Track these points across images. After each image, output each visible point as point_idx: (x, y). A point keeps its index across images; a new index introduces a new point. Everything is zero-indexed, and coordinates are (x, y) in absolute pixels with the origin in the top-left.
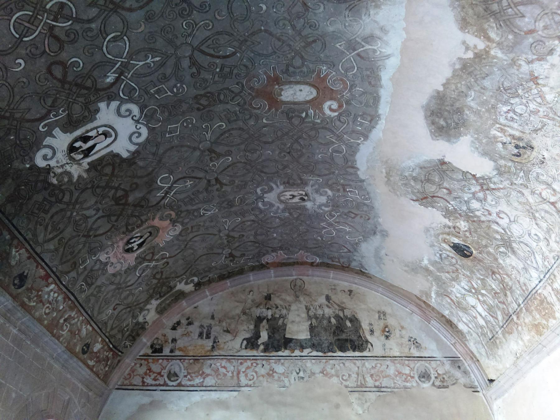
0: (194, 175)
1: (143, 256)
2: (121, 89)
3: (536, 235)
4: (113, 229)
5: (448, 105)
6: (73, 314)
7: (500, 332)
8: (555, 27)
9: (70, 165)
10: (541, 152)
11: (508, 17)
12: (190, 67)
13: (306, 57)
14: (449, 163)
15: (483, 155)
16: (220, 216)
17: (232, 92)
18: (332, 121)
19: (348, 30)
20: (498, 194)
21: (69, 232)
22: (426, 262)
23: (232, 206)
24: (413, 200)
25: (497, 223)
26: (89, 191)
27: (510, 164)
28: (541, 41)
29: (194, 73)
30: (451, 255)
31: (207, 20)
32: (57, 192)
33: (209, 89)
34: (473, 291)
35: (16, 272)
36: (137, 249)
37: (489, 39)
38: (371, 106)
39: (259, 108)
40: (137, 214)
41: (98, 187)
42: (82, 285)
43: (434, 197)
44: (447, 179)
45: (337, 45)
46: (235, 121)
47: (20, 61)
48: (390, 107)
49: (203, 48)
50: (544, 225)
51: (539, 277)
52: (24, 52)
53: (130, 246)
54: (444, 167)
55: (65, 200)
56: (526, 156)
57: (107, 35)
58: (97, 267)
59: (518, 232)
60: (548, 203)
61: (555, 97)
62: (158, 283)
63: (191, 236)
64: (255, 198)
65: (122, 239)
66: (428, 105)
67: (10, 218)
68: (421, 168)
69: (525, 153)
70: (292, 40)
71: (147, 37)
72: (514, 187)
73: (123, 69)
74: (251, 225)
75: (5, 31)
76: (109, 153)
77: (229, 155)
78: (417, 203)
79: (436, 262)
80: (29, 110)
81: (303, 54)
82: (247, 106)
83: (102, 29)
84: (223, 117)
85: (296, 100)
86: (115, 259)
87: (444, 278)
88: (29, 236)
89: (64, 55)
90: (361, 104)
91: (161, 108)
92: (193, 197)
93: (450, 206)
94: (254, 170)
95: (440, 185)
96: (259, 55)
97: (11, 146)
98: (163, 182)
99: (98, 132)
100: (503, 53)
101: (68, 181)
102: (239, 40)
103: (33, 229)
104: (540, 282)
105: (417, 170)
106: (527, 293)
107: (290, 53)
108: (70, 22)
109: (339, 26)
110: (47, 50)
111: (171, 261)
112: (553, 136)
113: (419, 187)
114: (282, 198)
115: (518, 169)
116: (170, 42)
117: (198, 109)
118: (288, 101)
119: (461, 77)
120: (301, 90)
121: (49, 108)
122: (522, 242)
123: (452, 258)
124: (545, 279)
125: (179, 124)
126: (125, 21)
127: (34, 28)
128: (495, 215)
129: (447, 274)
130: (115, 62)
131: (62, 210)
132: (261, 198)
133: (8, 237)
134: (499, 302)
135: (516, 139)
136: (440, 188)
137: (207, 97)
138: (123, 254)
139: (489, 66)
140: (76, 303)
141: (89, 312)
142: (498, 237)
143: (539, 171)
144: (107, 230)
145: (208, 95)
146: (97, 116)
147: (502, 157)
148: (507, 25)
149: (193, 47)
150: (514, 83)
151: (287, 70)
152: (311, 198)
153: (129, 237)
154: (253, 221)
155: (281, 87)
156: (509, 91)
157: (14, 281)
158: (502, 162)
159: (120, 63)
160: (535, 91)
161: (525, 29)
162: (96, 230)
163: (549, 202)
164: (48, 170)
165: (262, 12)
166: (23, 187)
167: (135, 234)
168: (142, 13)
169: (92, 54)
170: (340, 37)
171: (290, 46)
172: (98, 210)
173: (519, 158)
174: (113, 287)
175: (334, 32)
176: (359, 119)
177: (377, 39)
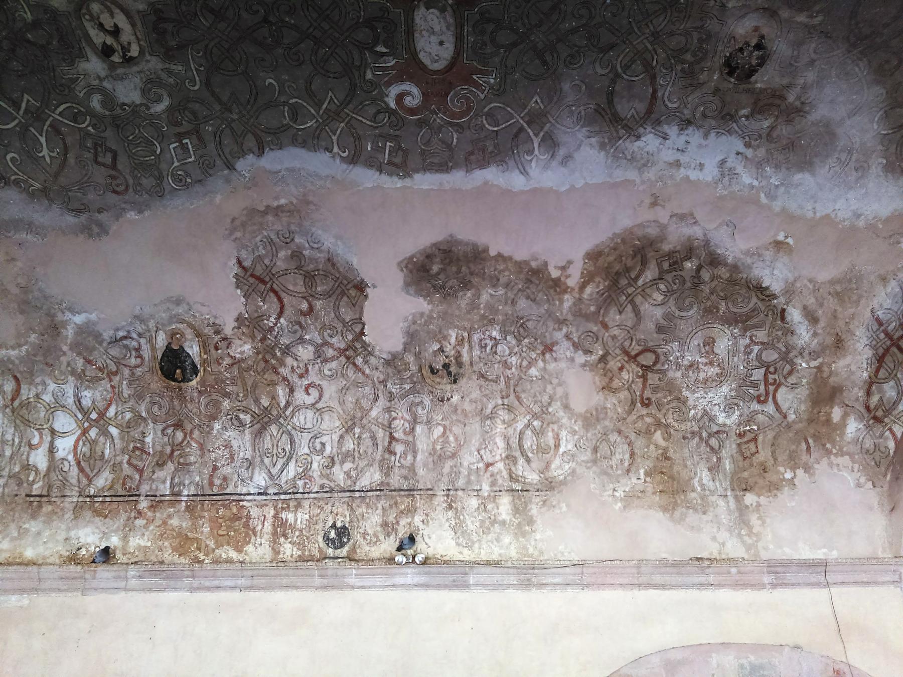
3: (323, 445)
5: (469, 268)
7: (75, 500)
8: (617, 345)
10: (455, 392)
11: (615, 299)
14: (366, 297)
15: (408, 332)
19: (563, 110)
20: (351, 372)
22: (79, 319)
24: (239, 262)
25: (292, 391)
27: (414, 368)
28: (597, 339)
30: (146, 353)
34: (94, 416)
37: (582, 287)
38: (424, 160)
43: (276, 293)
44: (329, 301)
45: (536, 98)
48: (432, 190)
50: (349, 445)
51: (267, 488)
54: (353, 292)
56: (438, 380)
59: (303, 422)
60: (388, 433)
61: (536, 377)
66: (458, 242)
68: (329, 260)
69: (442, 377)
72: (381, 387)
78: (236, 269)
79: (98, 337)
81: (522, 46)
85: (417, 35)
87: (64, 359)
90: (424, 144)
93: (272, 319)
95: (312, 296)
100: (570, 308)
104: (259, 494)
105: (321, 256)
106: (215, 490)
107: (524, 25)
112: (486, 396)
113: (281, 265)
115: (412, 380)
118: (413, 19)
119: (520, 272)
120: (441, 43)
122: (290, 434)
123: (140, 356)
124: (276, 497)
128: (307, 382)
129: (80, 363)
134: (129, 463)
135: (457, 361)
136: (305, 298)
139: (548, 300)
142: (265, 402)
143: (427, 401)
147: (418, 356)
148: (605, 300)
150: (535, 331)
152: (120, 71)
155: (449, 9)
156: (521, 330)
158: (410, 358)
160: (534, 356)
161: (606, 320)
163: (391, 433)
173: (429, 374)
176: (388, 144)
177: (551, 153)
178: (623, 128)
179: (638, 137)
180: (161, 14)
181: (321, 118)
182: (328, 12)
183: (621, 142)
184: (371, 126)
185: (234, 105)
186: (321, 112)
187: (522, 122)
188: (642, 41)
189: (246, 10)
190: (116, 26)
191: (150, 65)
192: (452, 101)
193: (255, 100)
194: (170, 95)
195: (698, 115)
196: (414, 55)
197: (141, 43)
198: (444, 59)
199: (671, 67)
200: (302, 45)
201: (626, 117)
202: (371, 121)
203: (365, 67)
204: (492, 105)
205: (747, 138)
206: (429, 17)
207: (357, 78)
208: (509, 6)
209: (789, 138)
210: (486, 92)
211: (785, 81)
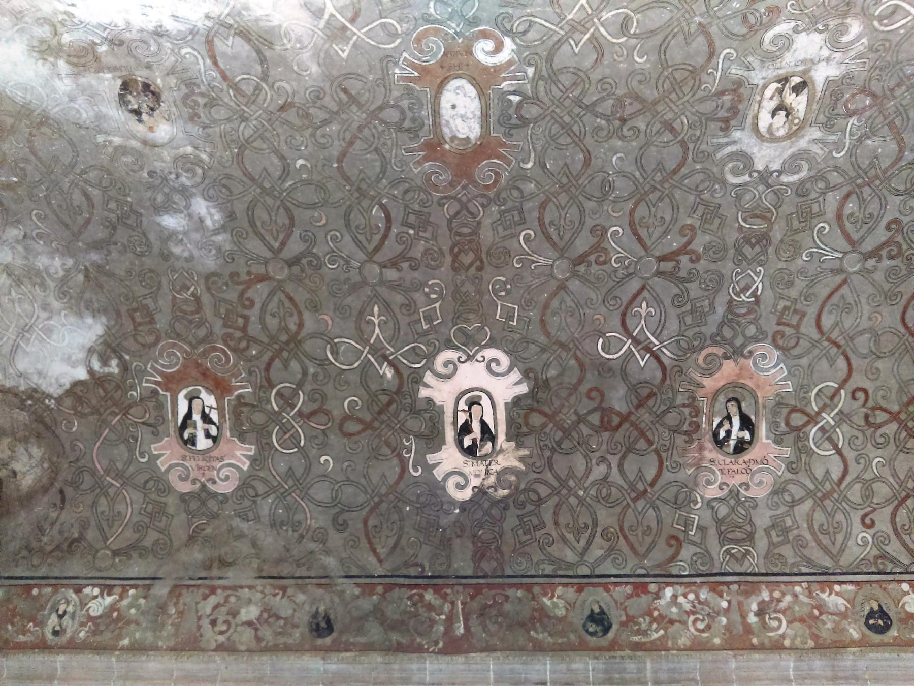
0: (625, 299)
1: (783, 427)
2: (408, 364)
4: (664, 455)
6: (765, 595)
9: (493, 463)
12: (399, 270)
13: (379, 103)
16: (781, 265)
17: (458, 213)
18: (527, 47)
19: (309, 43)
21: (606, 517)
23: (763, 239)
26: (556, 457)
29: (410, 265)
31: (326, 237)
32: (522, 497)
33: (446, 249)
35: (578, 618)
36: (752, 435)
39: (497, 174)
40: (663, 408)
41: (559, 443)
42: (728, 552)
46: (521, 211)
47: (323, 459)
49: (370, 248)
52: (314, 451)
53: (732, 443)
55: (543, 495)
57: (328, 359)
58: (723, 511)
62: (900, 422)
63: (808, 329)
64: (761, 188)
65: (701, 448)
67: (499, 573)
70: (350, 125)
71: (341, 316)
73: (379, 353)
74: (862, 201)
75: (287, 458)
76: (506, 409)
77: (605, 230)
80: (384, 475)
81: (372, 108)
82: (491, 194)
83: (318, 362)
84: (507, 232)
85: (478, 113)
86: (737, 476)
88: (549, 569)
89: (336, 413)
91: (458, 321)
92: (688, 307)
94: (667, 185)
96: (384, 171)
97: (417, 515)
98: (614, 351)
99: (463, 410)
101: (516, 476)
102: (357, 198)
103: (543, 557)
107: (375, 127)
108: (300, 393)
109: (306, 56)
110: (323, 428)
111: (858, 380)
114: (782, 133)
116: (355, 288)
117: (480, 269)
118: (482, 127)
120: (454, 107)
121: (395, 454)
125: (499, 302)
126: (313, 336)
127: (293, 430)
130: (365, 361)
131: (558, 506)
132: (765, 177)
133: (520, 593)
137: (460, 251)
138: (741, 461)
140: (750, 579)
141: (805, 570)
144: (657, 464)
145: (456, 250)
146: (438, 403)
149: (365, 261)
151: (409, 130)
153: (709, 436)
154: (847, 196)
155: (448, 140)
157: (587, 631)
159: (369, 356)
162: (640, 476)
164: (481, 492)
165: (309, 165)
166: (480, 532)
167: (710, 423)
168: (307, 315)
169: (347, 383)
170: (327, 52)
171: (360, 129)
172: (603, 460)
174: (809, 504)
175: (319, 64)
178: (231, 26)
179: (208, 17)
180: (723, 126)
181: (594, 24)
182: (561, 132)
183: (227, 12)
184: (535, 17)
185: (692, 31)
186: (592, 30)
187: (354, 30)
188: (255, 113)
189: (639, 130)
190: (774, 114)
191: (764, 74)
192: (439, 48)
193: (666, 37)
194: (761, 43)
195: (152, 42)
196: (481, 93)
197: (758, 98)
198: (448, 90)
199: (212, 88)
200: (595, 98)
201: (234, 37)
202: (536, 22)
203: (533, 78)
204: (392, 46)
205: (76, 21)
206: (466, 130)
207: (544, 68)
208: (392, 145)
209: (27, 23)
210: (402, 59)
211: (83, 80)
